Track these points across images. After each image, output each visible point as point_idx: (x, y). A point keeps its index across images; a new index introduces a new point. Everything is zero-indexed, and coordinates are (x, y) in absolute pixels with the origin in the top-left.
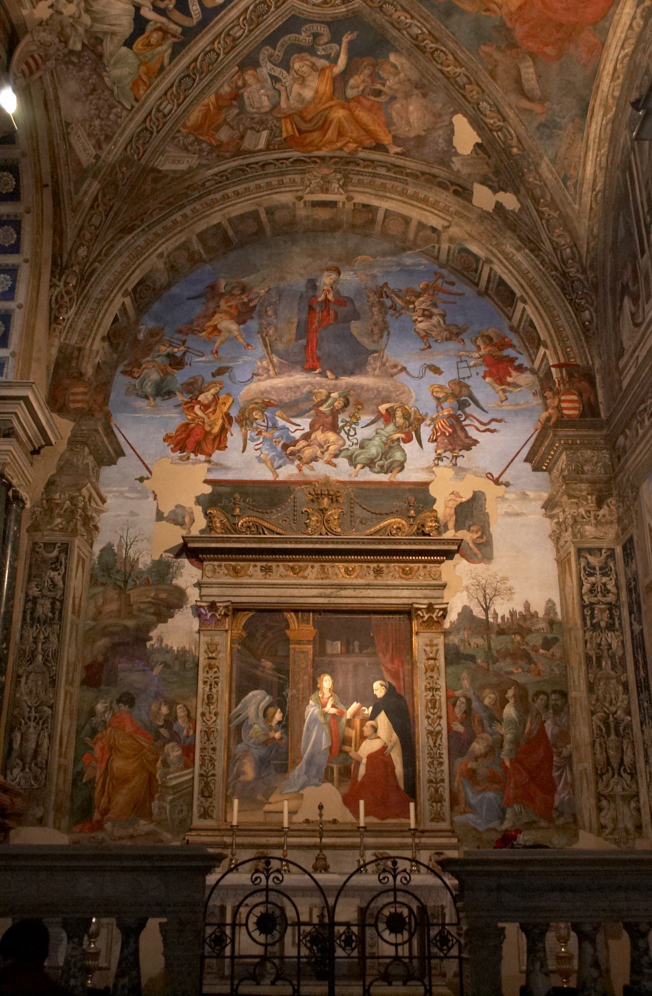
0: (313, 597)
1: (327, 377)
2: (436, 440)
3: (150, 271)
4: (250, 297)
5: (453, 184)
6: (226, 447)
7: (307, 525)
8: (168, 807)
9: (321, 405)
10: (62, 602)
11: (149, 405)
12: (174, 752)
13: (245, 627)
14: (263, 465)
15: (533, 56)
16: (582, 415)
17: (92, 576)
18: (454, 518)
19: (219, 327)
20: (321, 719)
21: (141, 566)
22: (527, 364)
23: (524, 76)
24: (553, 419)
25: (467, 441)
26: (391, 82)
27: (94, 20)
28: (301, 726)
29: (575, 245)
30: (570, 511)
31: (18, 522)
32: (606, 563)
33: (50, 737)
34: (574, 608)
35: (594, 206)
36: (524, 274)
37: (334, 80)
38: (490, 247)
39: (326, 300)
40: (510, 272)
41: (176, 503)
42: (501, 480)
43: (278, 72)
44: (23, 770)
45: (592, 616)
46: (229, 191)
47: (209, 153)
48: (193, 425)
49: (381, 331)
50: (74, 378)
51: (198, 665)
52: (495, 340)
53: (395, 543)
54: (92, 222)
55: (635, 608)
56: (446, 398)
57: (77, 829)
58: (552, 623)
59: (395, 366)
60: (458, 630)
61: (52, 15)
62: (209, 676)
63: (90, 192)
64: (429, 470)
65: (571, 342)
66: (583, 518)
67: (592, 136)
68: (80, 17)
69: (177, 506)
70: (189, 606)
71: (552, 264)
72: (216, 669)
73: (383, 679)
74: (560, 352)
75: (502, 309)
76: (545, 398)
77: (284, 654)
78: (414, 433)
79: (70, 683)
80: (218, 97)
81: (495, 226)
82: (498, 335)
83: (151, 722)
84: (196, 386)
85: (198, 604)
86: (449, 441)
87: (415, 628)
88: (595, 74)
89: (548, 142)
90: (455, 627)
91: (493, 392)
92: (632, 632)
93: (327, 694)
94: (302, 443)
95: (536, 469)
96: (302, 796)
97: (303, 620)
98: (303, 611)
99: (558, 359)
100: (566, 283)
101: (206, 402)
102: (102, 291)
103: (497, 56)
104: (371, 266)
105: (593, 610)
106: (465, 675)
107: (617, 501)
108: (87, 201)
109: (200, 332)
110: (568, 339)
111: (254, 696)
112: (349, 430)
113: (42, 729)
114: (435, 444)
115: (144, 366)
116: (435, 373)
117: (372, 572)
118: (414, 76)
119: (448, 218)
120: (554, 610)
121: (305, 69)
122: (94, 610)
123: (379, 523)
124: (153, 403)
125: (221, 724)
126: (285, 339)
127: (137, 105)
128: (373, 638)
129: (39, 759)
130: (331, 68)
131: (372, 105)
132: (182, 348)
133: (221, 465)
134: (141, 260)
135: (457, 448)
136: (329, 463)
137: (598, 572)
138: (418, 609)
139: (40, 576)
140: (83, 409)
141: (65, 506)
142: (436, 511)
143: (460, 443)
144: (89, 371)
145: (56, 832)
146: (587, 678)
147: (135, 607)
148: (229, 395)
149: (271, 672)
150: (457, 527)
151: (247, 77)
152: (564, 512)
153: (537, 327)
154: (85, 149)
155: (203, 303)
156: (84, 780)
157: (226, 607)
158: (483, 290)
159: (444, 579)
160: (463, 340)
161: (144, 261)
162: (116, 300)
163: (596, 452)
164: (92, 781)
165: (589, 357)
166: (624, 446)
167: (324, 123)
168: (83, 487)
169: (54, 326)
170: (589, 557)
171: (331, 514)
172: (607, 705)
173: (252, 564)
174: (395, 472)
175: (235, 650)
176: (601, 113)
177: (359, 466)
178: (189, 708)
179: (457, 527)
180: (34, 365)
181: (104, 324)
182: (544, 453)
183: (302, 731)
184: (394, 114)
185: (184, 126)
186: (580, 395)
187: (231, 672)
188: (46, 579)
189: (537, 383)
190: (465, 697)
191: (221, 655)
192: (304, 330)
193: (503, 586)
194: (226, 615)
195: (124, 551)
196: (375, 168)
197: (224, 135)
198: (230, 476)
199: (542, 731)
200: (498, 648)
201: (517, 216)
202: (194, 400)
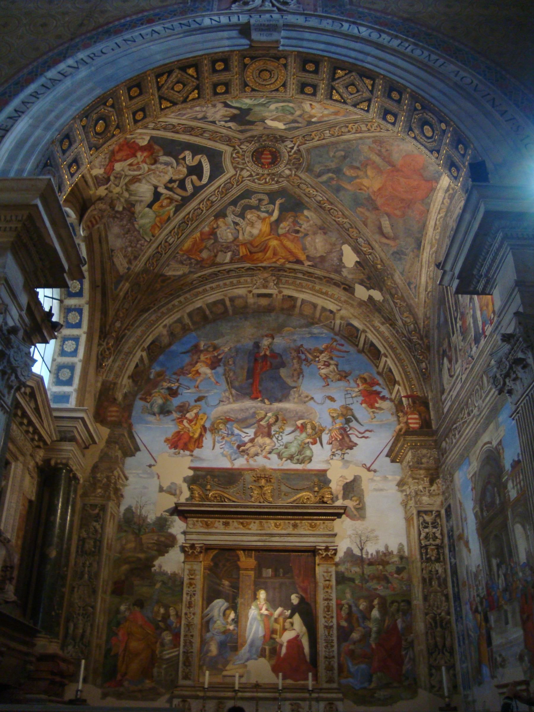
1: (265, 403)
2: (331, 443)
3: (159, 336)
4: (220, 352)
5: (343, 284)
7: (251, 496)
8: (163, 672)
12: (167, 637)
13: (213, 560)
14: (225, 458)
15: (388, 215)
16: (421, 427)
18: (342, 492)
19: (199, 371)
20: (259, 618)
21: (149, 520)
22: (387, 395)
23: (383, 225)
24: (403, 430)
25: (351, 444)
26: (305, 226)
27: (131, 195)
29: (416, 323)
30: (414, 488)
31: (75, 492)
32: (435, 520)
35: (427, 300)
36: (386, 340)
37: (271, 224)
38: (366, 323)
39: (265, 355)
40: (378, 338)
42: (371, 468)
43: (237, 220)
45: (427, 553)
46: (207, 287)
47: (197, 264)
49: (299, 375)
51: (183, 583)
52: (368, 381)
55: (452, 549)
56: (338, 417)
58: (402, 558)
59: (307, 397)
61: (107, 194)
63: (124, 289)
64: (327, 462)
65: (415, 382)
67: (424, 260)
68: (122, 193)
71: (403, 333)
73: (297, 593)
74: (407, 388)
76: (399, 417)
79: (105, 592)
80: (202, 233)
81: (368, 310)
82: (370, 377)
87: (317, 561)
88: (424, 227)
89: (399, 262)
90: (343, 561)
92: (451, 563)
94: (249, 445)
95: (393, 461)
96: (246, 666)
100: (411, 346)
101: (191, 418)
103: (368, 214)
104: (293, 334)
105: (427, 549)
106: (348, 591)
107: (442, 481)
108: (122, 294)
109: (188, 374)
111: (218, 603)
117: (291, 526)
118: (319, 222)
119: (340, 304)
120: (403, 550)
121: (254, 218)
123: (296, 495)
124: (158, 418)
125: (197, 620)
127: (153, 239)
130: (269, 218)
131: (294, 238)
132: (177, 384)
136: (266, 457)
137: (430, 526)
138: (320, 549)
141: (104, 482)
144: (120, 397)
146: (423, 591)
148: (205, 414)
149: (227, 588)
150: (345, 498)
151: (219, 223)
152: (410, 488)
153: (394, 373)
154: (121, 265)
157: (201, 547)
159: (336, 531)
160: (348, 380)
162: (137, 353)
164: (116, 655)
167: (265, 249)
170: (424, 515)
171: (267, 490)
172: (435, 609)
174: (306, 463)
176: (429, 248)
177: (284, 459)
179: (345, 498)
183: (246, 625)
184: (307, 243)
185: (181, 250)
186: (420, 415)
187: (204, 587)
189: (394, 407)
190: (348, 604)
191: (198, 577)
192: (251, 374)
193: (372, 535)
195: (139, 511)
196: (296, 273)
197: (205, 255)
198: (205, 465)
199: (395, 625)
200: (369, 573)
202: (183, 417)
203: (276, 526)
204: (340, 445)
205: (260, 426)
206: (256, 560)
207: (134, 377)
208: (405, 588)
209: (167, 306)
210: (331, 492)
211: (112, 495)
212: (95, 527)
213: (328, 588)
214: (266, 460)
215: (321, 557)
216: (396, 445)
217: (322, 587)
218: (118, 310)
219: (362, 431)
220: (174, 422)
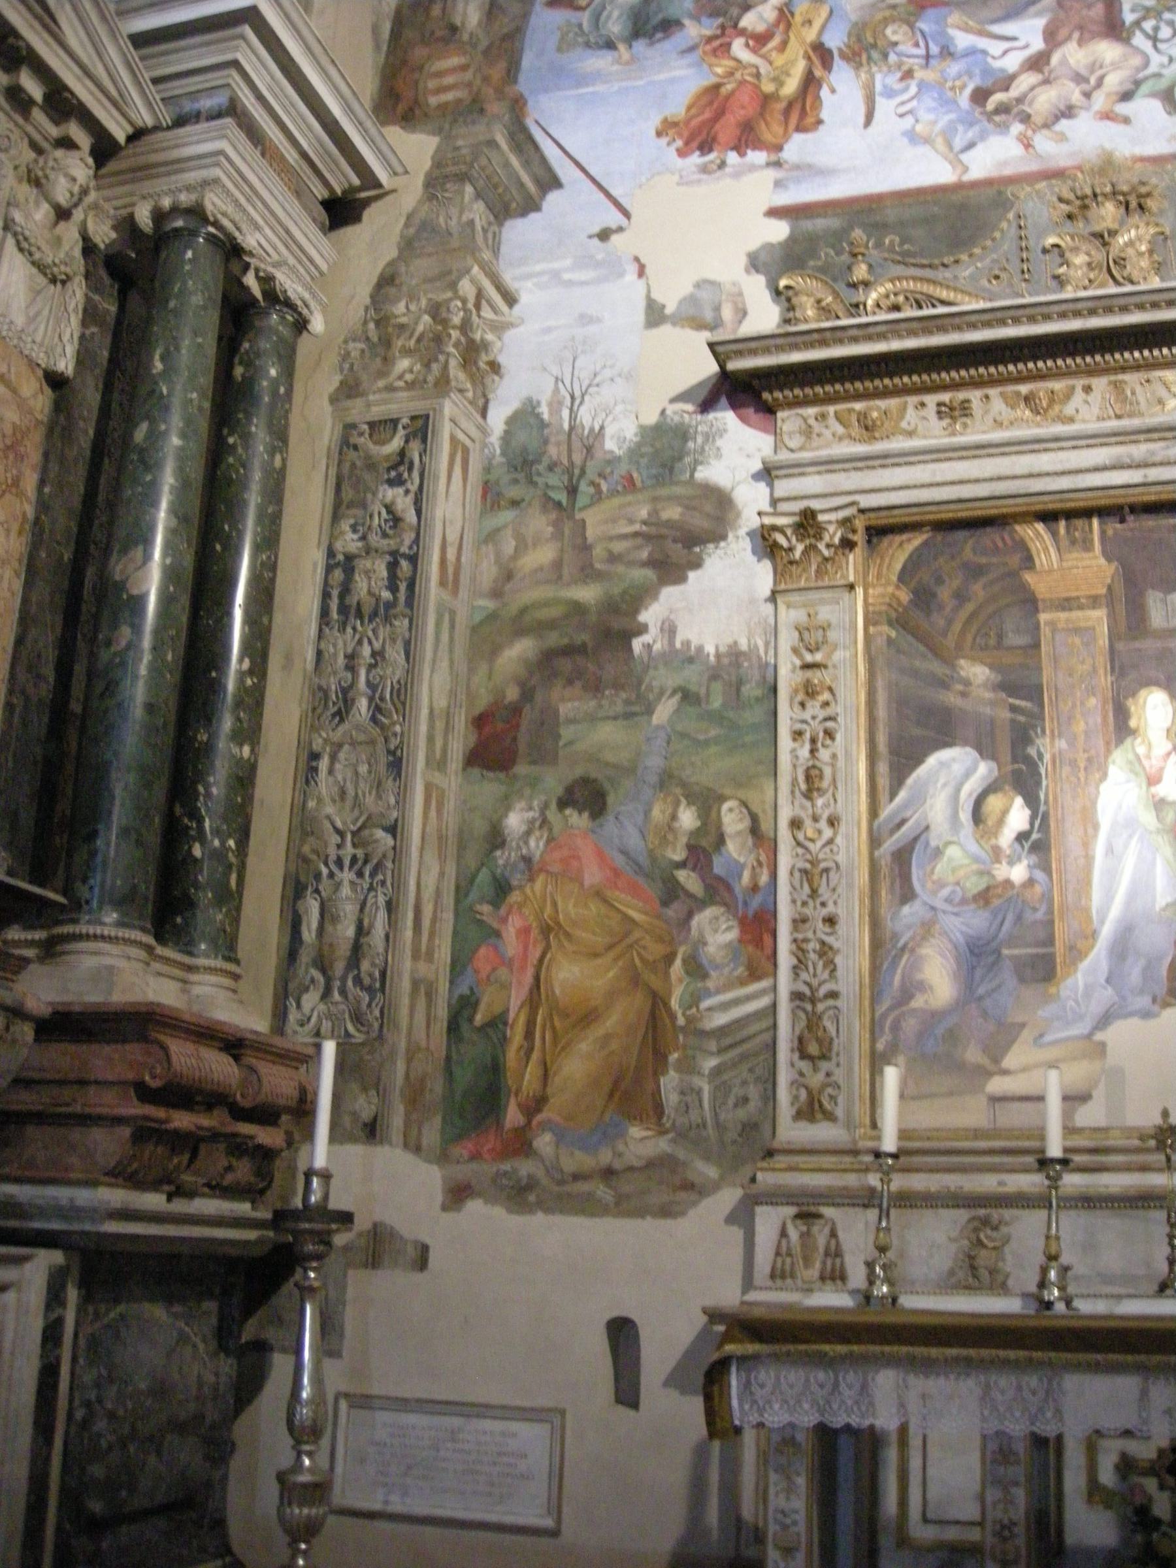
0: (1097, 469)
6: (820, 122)
10: (413, 559)
11: (618, 61)
13: (904, 576)
14: (925, 150)
17: (487, 488)
20: (1148, 818)
21: (610, 445)
28: (1087, 844)
33: (390, 906)
41: (696, 278)
44: (326, 995)
48: (729, 87)
50: (437, 40)
51: (775, 690)
57: (460, 1151)
62: (807, 715)
69: (698, 285)
70: (742, 532)
72: (826, 696)
77: (1022, 640)
79: (438, 763)
83: (651, 854)
85: (768, 521)
96: (1101, 1049)
97: (1073, 542)
98: (1070, 515)
101: (761, 28)
111: (942, 764)
112: (1156, 29)
113: (371, 888)
122: (494, 570)
129: (365, 966)
133: (810, 167)
136: (1108, 116)
139: (364, 505)
140: (459, 101)
141: (420, 328)
145: (409, 1158)
147: (598, 552)
149: (988, 695)
156: (479, 1019)
157: (846, 522)
168: (459, 278)
171: (1131, 243)
173: (912, 400)
175: (880, 642)
178: (755, 808)
183: (1089, 859)
188: (377, 507)
191: (839, 655)
194: (847, 544)
195: (565, 413)
202: (731, 28)
206: (1105, 553)
211: (456, 372)
212: (389, 508)
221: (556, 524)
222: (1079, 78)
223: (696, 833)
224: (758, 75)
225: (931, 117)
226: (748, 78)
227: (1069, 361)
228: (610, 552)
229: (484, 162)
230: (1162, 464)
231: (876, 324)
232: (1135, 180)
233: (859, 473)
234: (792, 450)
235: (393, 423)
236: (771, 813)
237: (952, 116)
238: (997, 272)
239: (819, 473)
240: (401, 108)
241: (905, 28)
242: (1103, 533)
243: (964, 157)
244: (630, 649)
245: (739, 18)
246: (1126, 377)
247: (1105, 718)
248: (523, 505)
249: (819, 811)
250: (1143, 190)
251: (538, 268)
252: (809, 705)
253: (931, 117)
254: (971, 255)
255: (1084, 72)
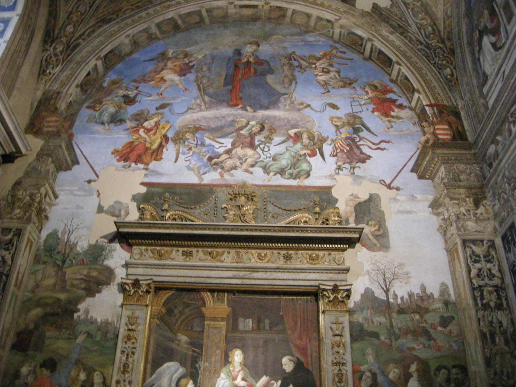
1: (247, 111)
2: (336, 155)
3: (119, 45)
4: (191, 59)
6: (162, 158)
7: (225, 218)
9: (242, 130)
10: (7, 276)
11: (104, 129)
13: (164, 305)
14: (192, 172)
16: (454, 138)
17: (36, 256)
18: (354, 214)
19: (165, 78)
24: (431, 142)
25: (362, 156)
29: (435, 24)
32: (488, 252)
34: (465, 290)
36: (398, 48)
38: (371, 32)
39: (248, 62)
40: (386, 46)
41: (116, 200)
42: (392, 185)
45: (482, 298)
48: (136, 143)
51: (118, 336)
52: (379, 88)
53: (302, 231)
54: (79, 9)
56: (343, 126)
58: (446, 303)
59: (302, 104)
60: (362, 310)
64: (332, 177)
65: (438, 90)
66: (464, 215)
69: (115, 202)
70: (116, 283)
71: (418, 40)
72: (134, 340)
73: (292, 355)
75: (383, 69)
76: (423, 127)
78: (317, 150)
82: (381, 85)
84: (142, 116)
85: (124, 281)
86: (347, 156)
87: (321, 307)
90: (360, 307)
91: (380, 122)
93: (238, 368)
95: (421, 177)
97: (219, 299)
98: (219, 291)
99: (430, 101)
101: (149, 127)
102: (82, 57)
104: (283, 41)
105: (482, 292)
106: (369, 351)
109: (150, 81)
110: (435, 88)
111: (169, 367)
112: (264, 148)
114: (336, 158)
115: (104, 103)
116: (334, 109)
117: (282, 258)
120: (448, 292)
122: (33, 283)
123: (289, 217)
126: (215, 86)
128: (282, 317)
132: (136, 92)
133: (156, 172)
134: (113, 39)
135: (354, 161)
136: (247, 171)
137: (482, 259)
140: (53, 131)
141: (25, 201)
142: (338, 208)
143: (356, 158)
144: (62, 106)
147: (68, 283)
148: (168, 122)
149: (186, 346)
150: (357, 221)
152: (448, 210)
155: (156, 64)
157: (148, 285)
158: (368, 56)
159: (347, 264)
160: (354, 88)
161: (115, 40)
163: (468, 166)
165: (453, 100)
166: (496, 151)
168: (42, 186)
169: (41, 76)
170: (472, 246)
171: (247, 210)
174: (302, 178)
175: (154, 324)
177: (272, 174)
178: (106, 375)
180: (15, 92)
181: (79, 77)
182: (426, 166)
186: (450, 125)
189: (415, 116)
190: (370, 371)
191: (140, 327)
193: (400, 271)
194: (148, 292)
195: (66, 236)
200: (400, 325)
201: (389, 10)
202: (140, 125)
203: (260, 257)
204: (348, 158)
205: (239, 136)
206: (228, 305)
207: (83, 86)
208: (455, 348)
209: (133, 18)
210: (339, 213)
213: (339, 346)
214: (247, 174)
215: (326, 300)
216: (424, 159)
217: (331, 346)
218: (71, 13)
219: (376, 140)
220: (127, 132)
221: (57, 272)
222: (240, 158)
223: (85, 381)
224: (146, 141)
225: (195, 163)
226: (143, 141)
227: (224, 243)
228: (72, 284)
229: (57, 152)
230: (248, 279)
231: (167, 224)
232: (252, 191)
233: (155, 270)
234: (135, 259)
235: (9, 230)
236: (110, 377)
237: (201, 163)
238: (207, 213)
239: (143, 268)
240: (34, 130)
241: (192, 135)
242: (228, 298)
243: (202, 176)
244: (73, 317)
245: (143, 123)
246: (241, 250)
247: (221, 356)
248: (47, 264)
249: (126, 378)
250: (253, 194)
251: (67, 188)
252: (128, 342)
253: (195, 163)
254: (200, 207)
255: (242, 157)
